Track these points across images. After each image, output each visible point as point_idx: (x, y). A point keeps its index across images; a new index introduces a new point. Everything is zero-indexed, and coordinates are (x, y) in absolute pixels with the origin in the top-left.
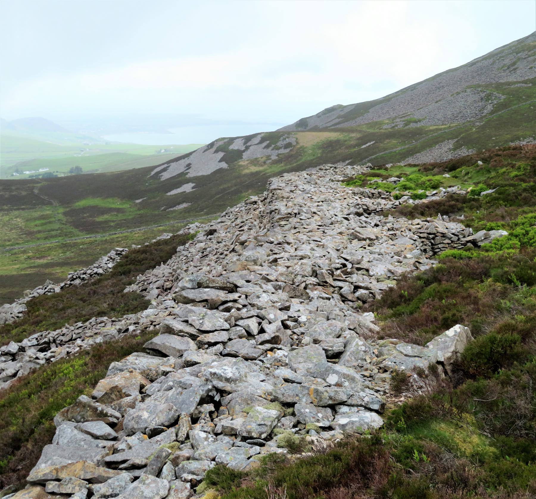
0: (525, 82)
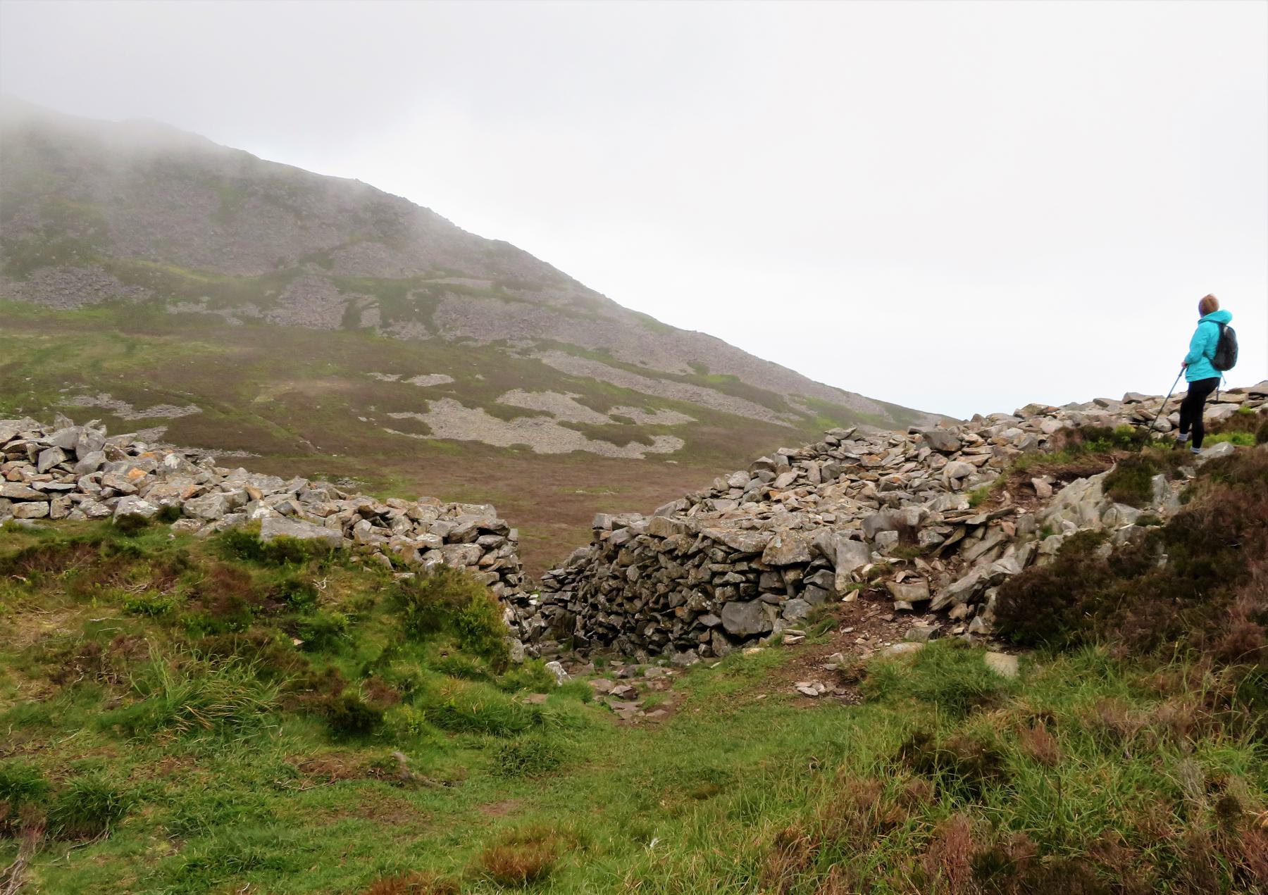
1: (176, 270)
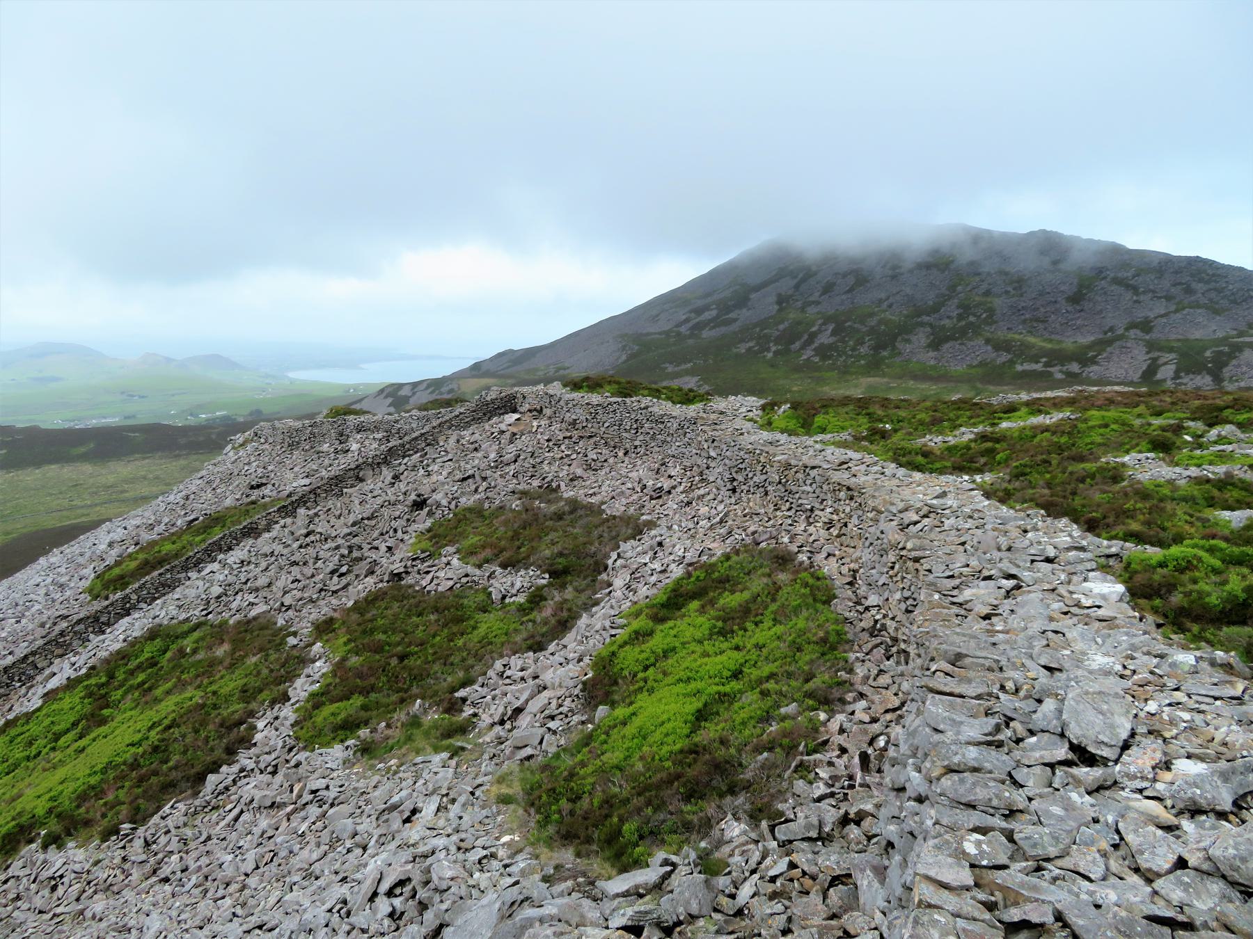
0: (660, 333)
1: (1032, 340)
